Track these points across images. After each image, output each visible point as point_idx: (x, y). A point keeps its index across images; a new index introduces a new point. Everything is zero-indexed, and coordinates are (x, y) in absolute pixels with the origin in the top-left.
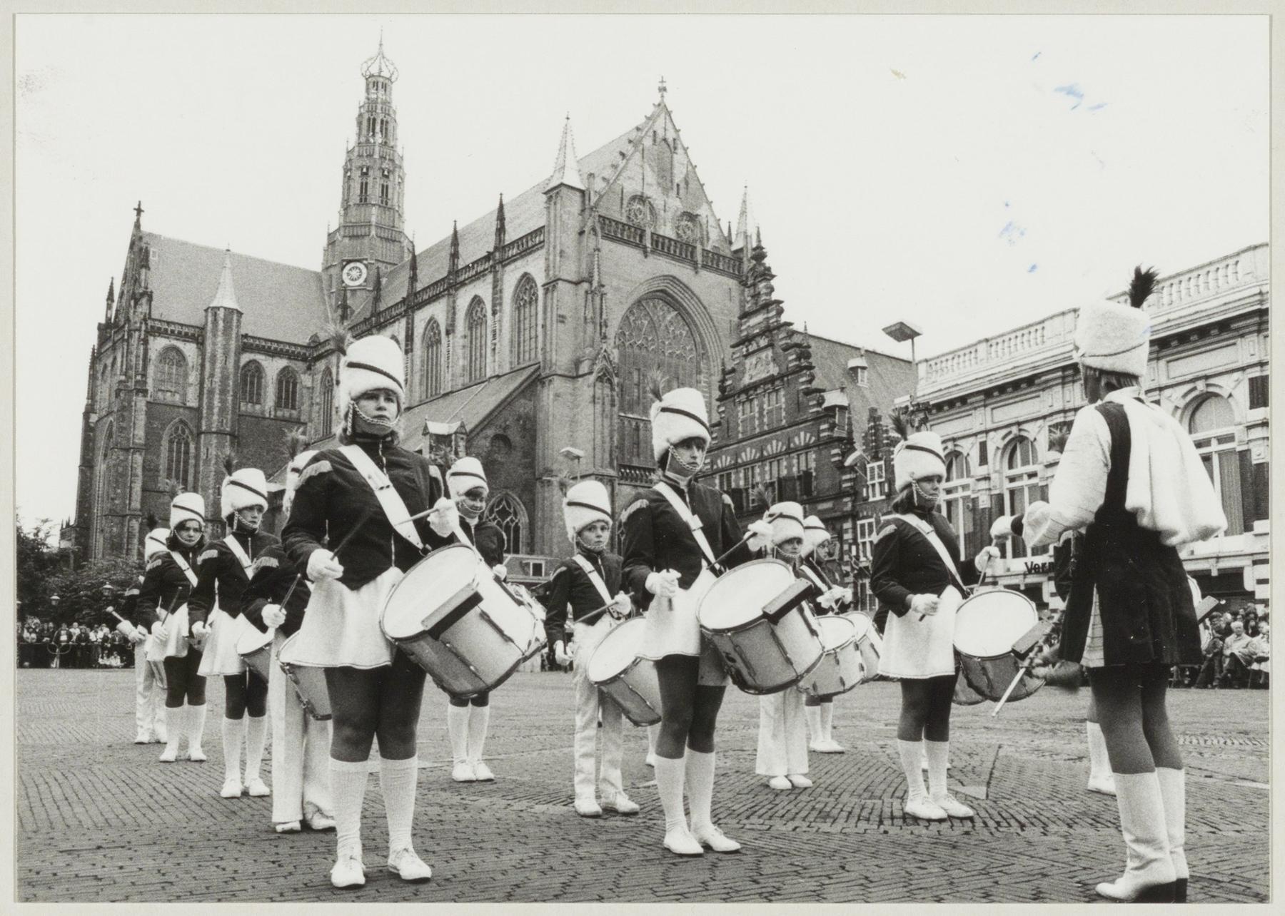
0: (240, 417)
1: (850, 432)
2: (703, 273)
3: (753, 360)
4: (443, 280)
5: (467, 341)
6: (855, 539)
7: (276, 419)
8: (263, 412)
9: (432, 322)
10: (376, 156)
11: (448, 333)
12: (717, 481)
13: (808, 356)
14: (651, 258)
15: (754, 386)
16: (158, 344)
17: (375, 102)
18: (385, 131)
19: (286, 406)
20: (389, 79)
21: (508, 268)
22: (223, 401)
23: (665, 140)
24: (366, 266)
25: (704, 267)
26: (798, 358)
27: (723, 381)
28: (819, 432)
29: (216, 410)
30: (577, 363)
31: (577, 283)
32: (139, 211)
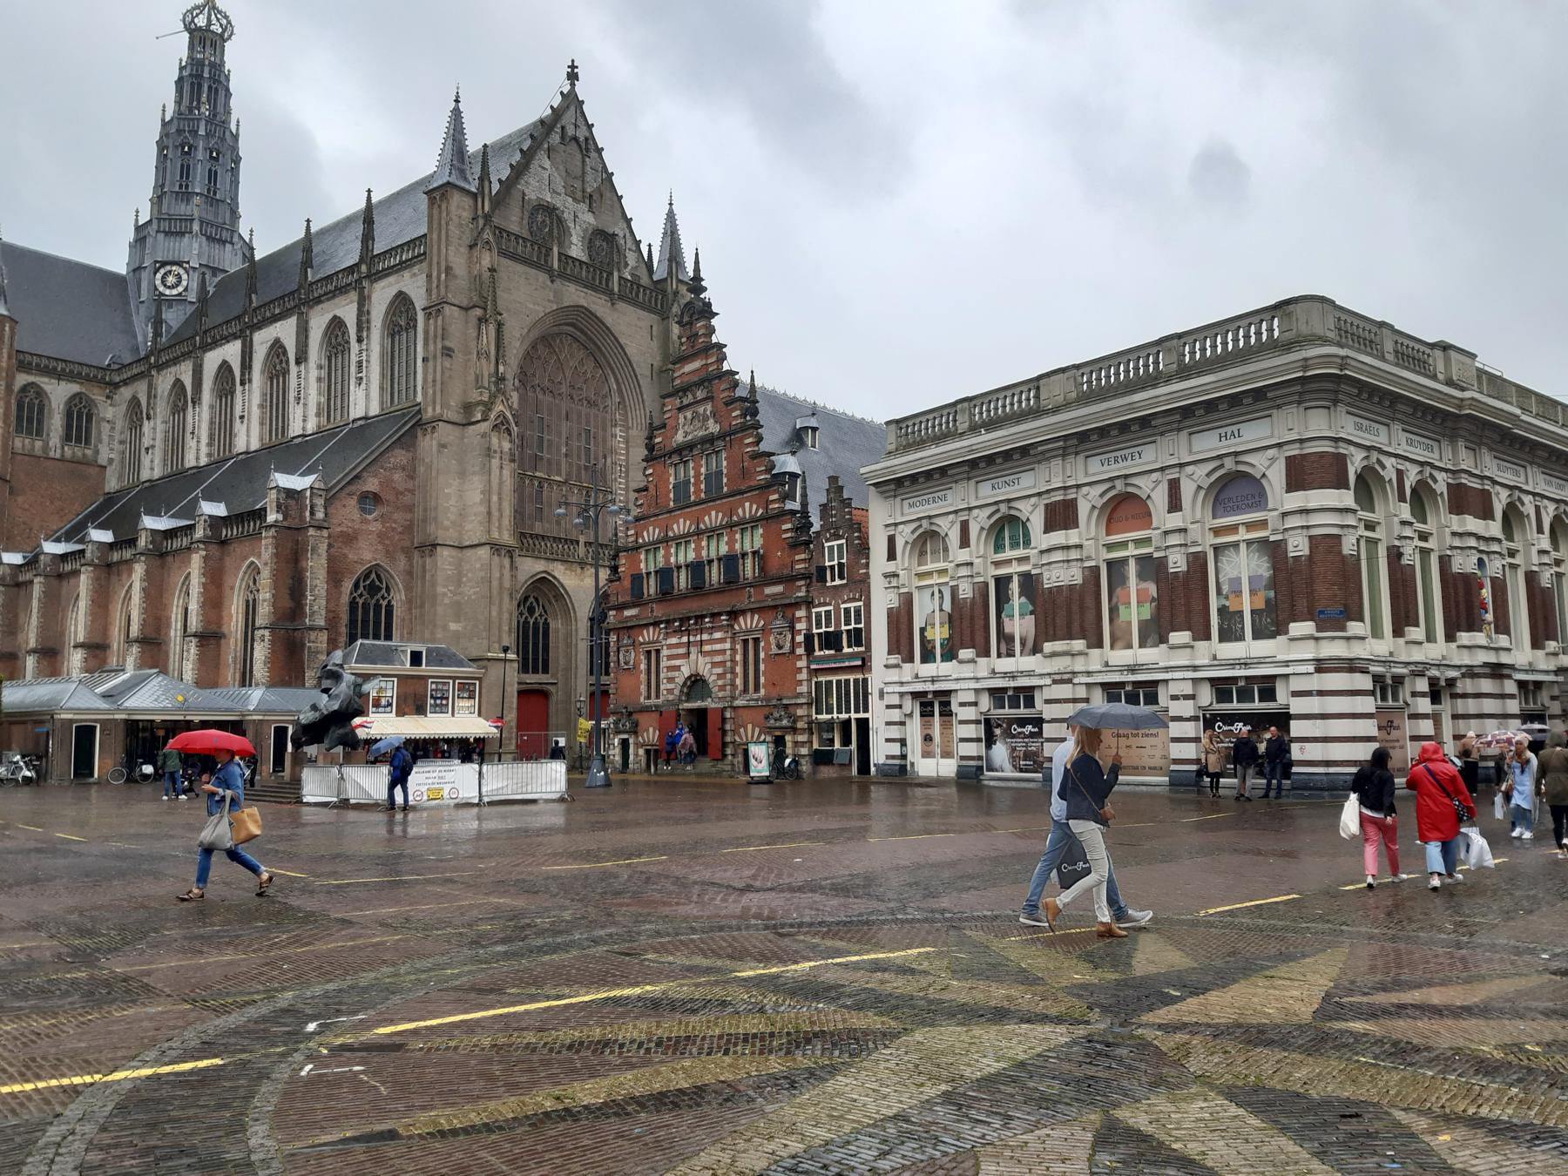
1: (804, 504)
2: (621, 305)
3: (689, 415)
4: (292, 293)
5: (324, 373)
6: (809, 629)
7: (62, 460)
8: (46, 447)
9: (277, 347)
10: (202, 132)
11: (298, 363)
12: (642, 557)
13: (755, 413)
14: (558, 281)
15: (690, 446)
17: (201, 63)
18: (212, 100)
19: (79, 440)
20: (221, 35)
21: (379, 285)
23: (575, 139)
24: (187, 272)
25: (622, 298)
26: (744, 415)
27: (650, 438)
28: (768, 502)
30: (468, 408)
31: (466, 309)
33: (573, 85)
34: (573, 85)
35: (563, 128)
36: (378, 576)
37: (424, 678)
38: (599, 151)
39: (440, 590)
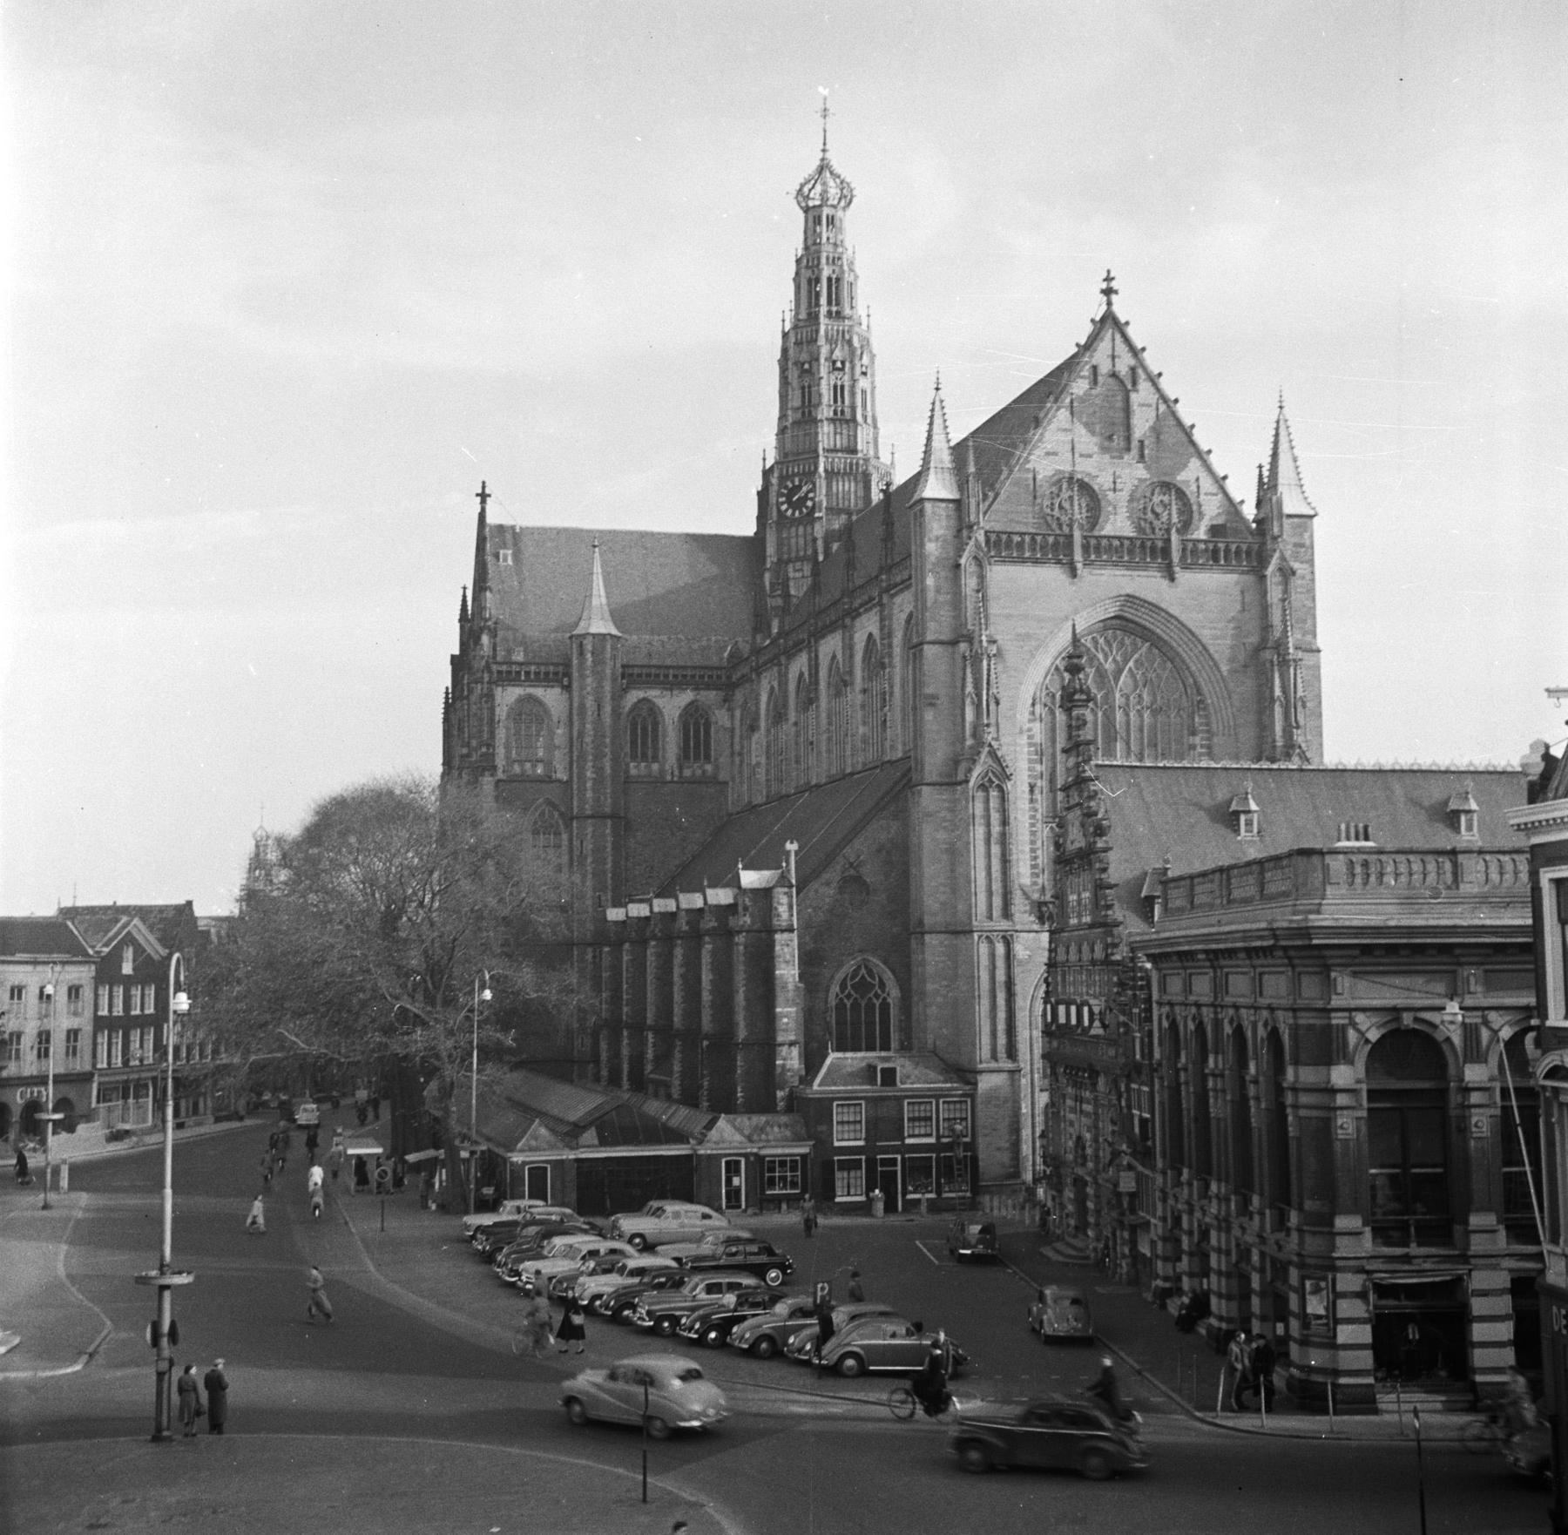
2: (1184, 577)
7: (682, 781)
8: (662, 771)
16: (507, 697)
18: (835, 298)
22: (599, 770)
29: (589, 785)
32: (483, 496)
33: (1109, 304)
34: (1109, 304)
35: (1095, 368)
36: (870, 972)
37: (899, 1099)
38: (1154, 380)
39: (930, 987)
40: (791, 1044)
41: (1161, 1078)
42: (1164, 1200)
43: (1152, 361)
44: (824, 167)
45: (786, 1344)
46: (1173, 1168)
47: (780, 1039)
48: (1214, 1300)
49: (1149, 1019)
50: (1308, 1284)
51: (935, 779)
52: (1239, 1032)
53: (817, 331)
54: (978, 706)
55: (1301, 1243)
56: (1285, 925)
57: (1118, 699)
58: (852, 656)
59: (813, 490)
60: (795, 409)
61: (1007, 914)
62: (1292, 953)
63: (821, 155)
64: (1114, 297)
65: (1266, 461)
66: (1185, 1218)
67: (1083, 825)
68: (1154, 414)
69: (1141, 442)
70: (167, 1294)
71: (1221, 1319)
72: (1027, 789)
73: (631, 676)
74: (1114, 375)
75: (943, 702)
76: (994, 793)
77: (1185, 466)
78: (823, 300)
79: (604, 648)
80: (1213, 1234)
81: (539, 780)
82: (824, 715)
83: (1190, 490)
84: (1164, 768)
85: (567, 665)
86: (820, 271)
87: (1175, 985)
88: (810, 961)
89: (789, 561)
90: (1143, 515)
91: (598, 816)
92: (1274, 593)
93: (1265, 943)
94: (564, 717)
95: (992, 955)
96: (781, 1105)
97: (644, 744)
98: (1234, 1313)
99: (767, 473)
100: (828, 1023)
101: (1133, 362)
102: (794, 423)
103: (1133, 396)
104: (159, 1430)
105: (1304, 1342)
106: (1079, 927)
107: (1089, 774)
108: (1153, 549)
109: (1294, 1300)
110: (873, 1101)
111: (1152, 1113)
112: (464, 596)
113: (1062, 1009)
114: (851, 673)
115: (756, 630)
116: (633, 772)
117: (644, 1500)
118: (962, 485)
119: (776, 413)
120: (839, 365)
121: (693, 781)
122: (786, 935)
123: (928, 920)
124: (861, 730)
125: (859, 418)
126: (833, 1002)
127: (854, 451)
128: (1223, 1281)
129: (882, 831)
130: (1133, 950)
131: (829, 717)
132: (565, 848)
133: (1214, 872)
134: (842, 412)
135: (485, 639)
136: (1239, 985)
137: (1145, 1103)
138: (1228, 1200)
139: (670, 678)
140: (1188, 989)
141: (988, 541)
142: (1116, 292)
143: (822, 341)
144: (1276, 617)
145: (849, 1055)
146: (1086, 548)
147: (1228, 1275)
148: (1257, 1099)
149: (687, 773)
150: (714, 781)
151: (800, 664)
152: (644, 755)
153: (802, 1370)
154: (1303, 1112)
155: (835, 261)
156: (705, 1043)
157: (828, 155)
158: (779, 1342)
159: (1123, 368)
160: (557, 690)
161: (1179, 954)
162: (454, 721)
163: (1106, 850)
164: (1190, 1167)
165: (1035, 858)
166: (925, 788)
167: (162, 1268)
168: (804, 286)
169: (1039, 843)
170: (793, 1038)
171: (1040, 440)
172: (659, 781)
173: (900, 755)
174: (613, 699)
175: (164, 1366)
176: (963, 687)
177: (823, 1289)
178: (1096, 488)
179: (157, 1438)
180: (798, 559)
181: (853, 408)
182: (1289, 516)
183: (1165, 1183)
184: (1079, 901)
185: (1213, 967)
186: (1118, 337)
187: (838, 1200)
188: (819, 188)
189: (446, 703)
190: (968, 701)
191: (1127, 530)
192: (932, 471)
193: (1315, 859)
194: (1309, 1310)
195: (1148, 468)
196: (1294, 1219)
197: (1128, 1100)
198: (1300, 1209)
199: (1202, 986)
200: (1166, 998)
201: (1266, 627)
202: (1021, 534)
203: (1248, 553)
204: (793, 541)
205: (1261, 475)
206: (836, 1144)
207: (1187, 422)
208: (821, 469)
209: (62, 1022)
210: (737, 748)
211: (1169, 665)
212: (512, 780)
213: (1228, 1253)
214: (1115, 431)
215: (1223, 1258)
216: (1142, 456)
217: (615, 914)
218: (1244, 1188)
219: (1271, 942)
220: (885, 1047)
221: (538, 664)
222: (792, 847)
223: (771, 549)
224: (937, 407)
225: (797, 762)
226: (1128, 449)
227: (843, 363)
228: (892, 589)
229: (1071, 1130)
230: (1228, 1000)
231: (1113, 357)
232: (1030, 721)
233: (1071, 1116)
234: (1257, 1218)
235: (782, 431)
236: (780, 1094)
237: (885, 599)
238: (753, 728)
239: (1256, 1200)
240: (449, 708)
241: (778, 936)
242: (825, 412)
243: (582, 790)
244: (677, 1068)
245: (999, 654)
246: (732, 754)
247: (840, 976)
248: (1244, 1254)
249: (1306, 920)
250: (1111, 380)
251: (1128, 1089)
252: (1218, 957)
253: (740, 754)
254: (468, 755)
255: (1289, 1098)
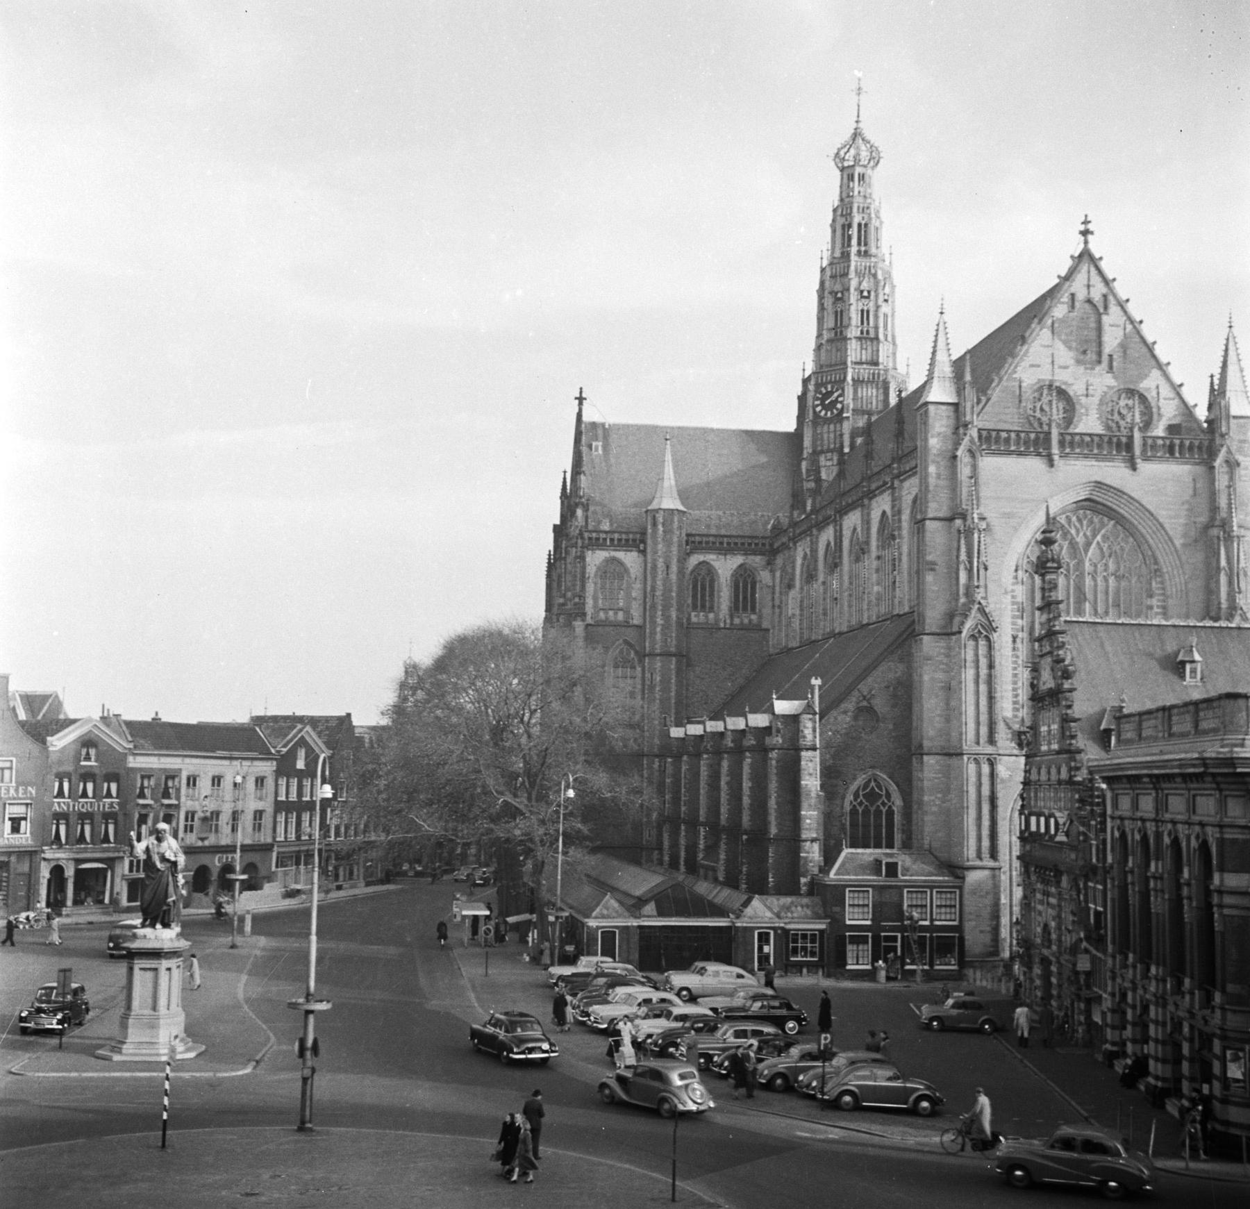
0: (686, 628)
2: (1145, 468)
7: (732, 628)
8: (717, 620)
16: (595, 559)
18: (863, 240)
19: (745, 609)
22: (667, 618)
29: (658, 629)
32: (581, 399)
33: (1086, 242)
34: (1086, 242)
35: (1073, 295)
37: (900, 888)
38: (1122, 305)
39: (926, 798)
40: (813, 840)
41: (1113, 879)
42: (1113, 979)
43: (1122, 291)
44: (856, 135)
45: (796, 1081)
46: (1121, 953)
47: (804, 836)
48: (1151, 1062)
49: (1104, 830)
50: (1229, 1053)
51: (934, 629)
52: (1176, 842)
53: (849, 266)
54: (970, 571)
55: (1224, 1019)
56: (1214, 755)
57: (1088, 567)
58: (869, 529)
59: (842, 395)
60: (829, 330)
61: (991, 740)
62: (1219, 779)
63: (855, 125)
64: (1090, 237)
65: (1217, 371)
66: (1130, 995)
67: (1052, 670)
68: (1122, 333)
69: (1110, 356)
70: (311, 1018)
71: (1157, 1078)
72: (1011, 639)
73: (694, 543)
74: (1089, 301)
75: (941, 569)
76: (982, 643)
77: (1147, 376)
78: (854, 241)
79: (672, 521)
80: (1152, 1008)
81: (616, 625)
82: (846, 578)
83: (1151, 396)
84: (1123, 624)
85: (644, 533)
86: (852, 218)
87: (1125, 803)
88: (830, 774)
89: (822, 452)
90: (1111, 416)
91: (666, 654)
92: (1222, 481)
93: (1197, 770)
94: (640, 576)
95: (979, 775)
96: (804, 889)
97: (703, 596)
98: (1168, 1074)
99: (805, 382)
100: (844, 825)
101: (1105, 290)
102: (828, 341)
103: (1104, 318)
104: (303, 1122)
105: (1225, 1101)
106: (1049, 752)
107: (1057, 628)
108: (1119, 445)
109: (1217, 1068)
110: (879, 889)
111: (1105, 906)
112: (565, 479)
113: (1033, 819)
114: (867, 543)
115: (793, 507)
116: (694, 619)
117: (164, 1146)
118: (960, 391)
119: (815, 334)
120: (865, 294)
121: (742, 628)
122: (810, 753)
123: (926, 744)
124: (876, 588)
125: (881, 336)
126: (847, 808)
127: (876, 364)
128: (1160, 1047)
129: (889, 671)
130: (1091, 773)
131: (850, 578)
132: (638, 681)
133: (1158, 710)
134: (868, 332)
135: (579, 512)
136: (1177, 804)
137: (1099, 901)
138: (1164, 981)
139: (725, 546)
140: (1135, 806)
141: (980, 437)
142: (1092, 233)
143: (852, 275)
144: (1223, 502)
145: (860, 851)
146: (1062, 444)
147: (1164, 1043)
148: (1190, 898)
149: (737, 621)
150: (758, 628)
151: (828, 535)
152: (703, 606)
153: (808, 1102)
154: (1226, 911)
155: (863, 210)
156: (745, 837)
157: (860, 125)
158: (791, 1078)
159: (1096, 295)
160: (635, 554)
161: (1129, 777)
162: (555, 577)
163: (1071, 691)
164: (1134, 953)
165: (1016, 696)
166: (925, 637)
167: (308, 996)
168: (839, 233)
169: (1020, 684)
170: (815, 835)
171: (1025, 354)
172: (713, 628)
173: (907, 609)
174: (679, 561)
175: (307, 1072)
176: (958, 557)
177: (826, 1039)
178: (1071, 393)
179: (302, 1129)
180: (829, 451)
181: (876, 328)
182: (1234, 417)
183: (1114, 965)
184: (1049, 731)
185: (1155, 788)
186: (1093, 269)
187: (848, 967)
188: (852, 151)
189: (549, 563)
190: (962, 567)
191: (1098, 429)
192: (935, 381)
193: (1241, 702)
194: (1229, 1075)
195: (1115, 378)
196: (1218, 998)
197: (1086, 895)
198: (1223, 991)
199: (1147, 804)
200: (1118, 813)
201: (1214, 509)
202: (1008, 431)
203: (1200, 448)
204: (825, 436)
205: (1212, 384)
206: (848, 922)
207: (1150, 339)
208: (849, 378)
209: (252, 805)
210: (777, 602)
211: (1131, 539)
212: (598, 624)
213: (1164, 1024)
214: (1090, 348)
215: (1160, 1029)
216: (1111, 367)
217: (676, 732)
218: (1178, 971)
219: (1202, 770)
220: (890, 846)
221: (620, 533)
222: (816, 682)
223: (807, 442)
224: (941, 328)
225: (825, 614)
226: (1099, 362)
227: (869, 292)
228: (902, 475)
229: (1039, 919)
230: (1167, 816)
231: (1089, 286)
232: (1014, 584)
233: (1040, 907)
234: (1187, 997)
235: (819, 348)
236: (803, 880)
237: (896, 483)
238: (790, 586)
239: (1187, 981)
240: (551, 567)
241: (803, 754)
242: (853, 332)
243: (653, 633)
244: (722, 856)
245: (988, 529)
246: (773, 606)
247: (853, 788)
248: (1177, 1026)
249: (1231, 752)
250: (1087, 306)
251: (1086, 887)
252: (1159, 781)
253: (779, 607)
254: (563, 605)
255: (1215, 899)
